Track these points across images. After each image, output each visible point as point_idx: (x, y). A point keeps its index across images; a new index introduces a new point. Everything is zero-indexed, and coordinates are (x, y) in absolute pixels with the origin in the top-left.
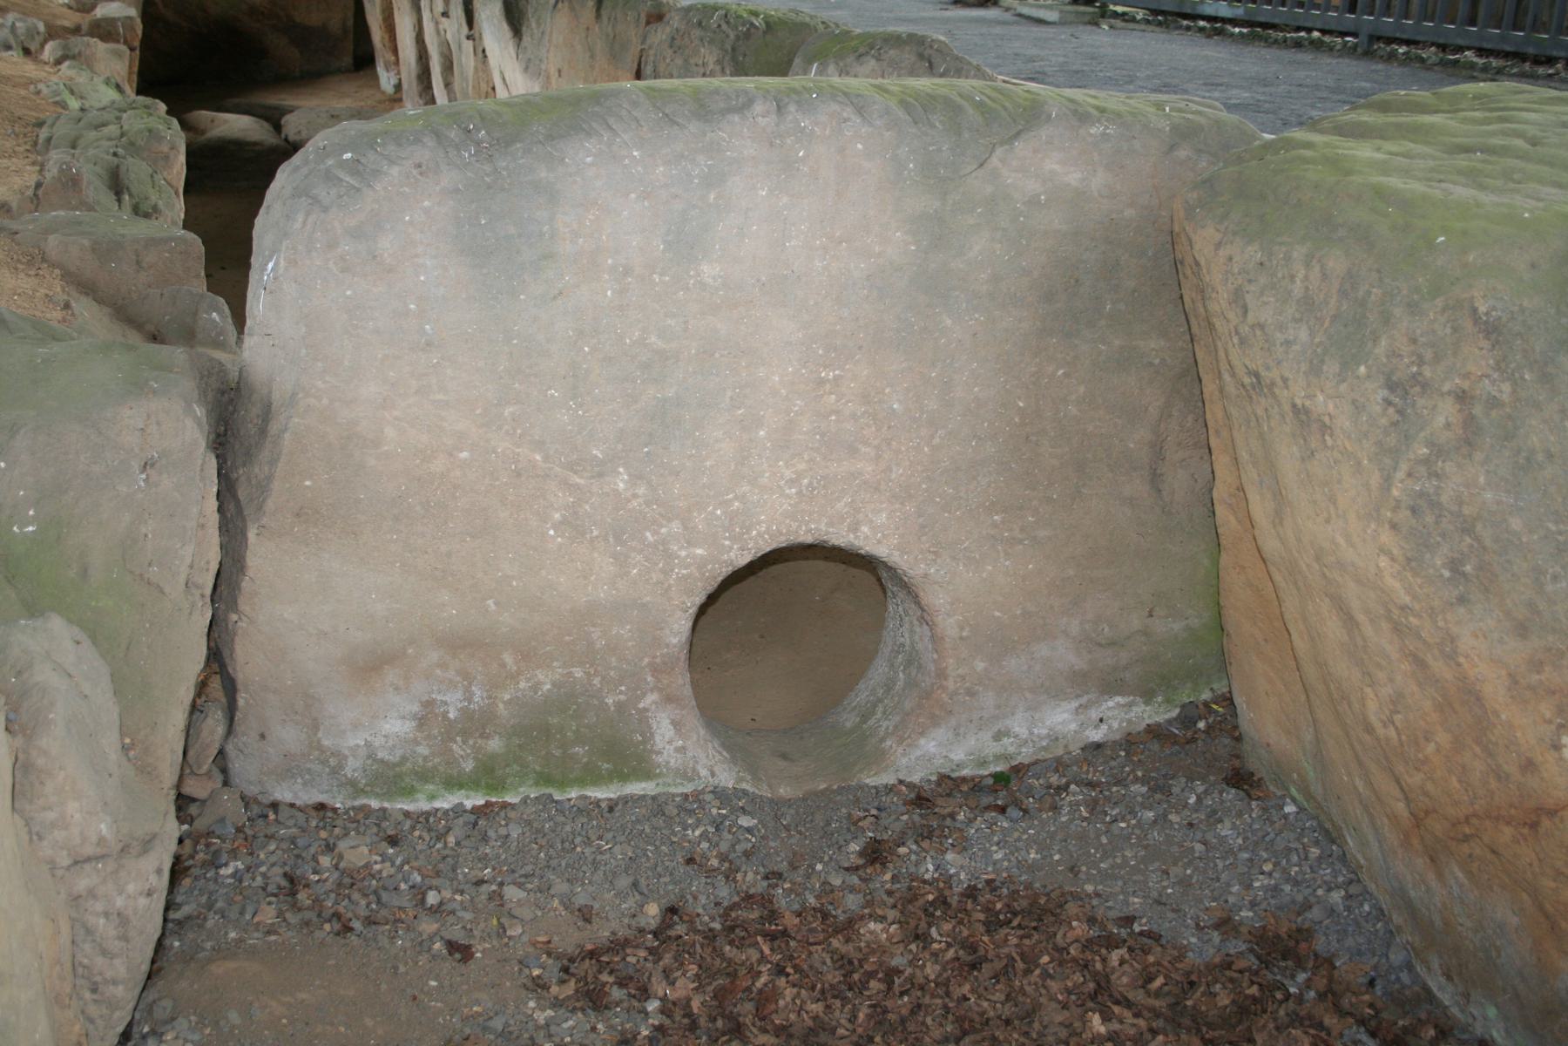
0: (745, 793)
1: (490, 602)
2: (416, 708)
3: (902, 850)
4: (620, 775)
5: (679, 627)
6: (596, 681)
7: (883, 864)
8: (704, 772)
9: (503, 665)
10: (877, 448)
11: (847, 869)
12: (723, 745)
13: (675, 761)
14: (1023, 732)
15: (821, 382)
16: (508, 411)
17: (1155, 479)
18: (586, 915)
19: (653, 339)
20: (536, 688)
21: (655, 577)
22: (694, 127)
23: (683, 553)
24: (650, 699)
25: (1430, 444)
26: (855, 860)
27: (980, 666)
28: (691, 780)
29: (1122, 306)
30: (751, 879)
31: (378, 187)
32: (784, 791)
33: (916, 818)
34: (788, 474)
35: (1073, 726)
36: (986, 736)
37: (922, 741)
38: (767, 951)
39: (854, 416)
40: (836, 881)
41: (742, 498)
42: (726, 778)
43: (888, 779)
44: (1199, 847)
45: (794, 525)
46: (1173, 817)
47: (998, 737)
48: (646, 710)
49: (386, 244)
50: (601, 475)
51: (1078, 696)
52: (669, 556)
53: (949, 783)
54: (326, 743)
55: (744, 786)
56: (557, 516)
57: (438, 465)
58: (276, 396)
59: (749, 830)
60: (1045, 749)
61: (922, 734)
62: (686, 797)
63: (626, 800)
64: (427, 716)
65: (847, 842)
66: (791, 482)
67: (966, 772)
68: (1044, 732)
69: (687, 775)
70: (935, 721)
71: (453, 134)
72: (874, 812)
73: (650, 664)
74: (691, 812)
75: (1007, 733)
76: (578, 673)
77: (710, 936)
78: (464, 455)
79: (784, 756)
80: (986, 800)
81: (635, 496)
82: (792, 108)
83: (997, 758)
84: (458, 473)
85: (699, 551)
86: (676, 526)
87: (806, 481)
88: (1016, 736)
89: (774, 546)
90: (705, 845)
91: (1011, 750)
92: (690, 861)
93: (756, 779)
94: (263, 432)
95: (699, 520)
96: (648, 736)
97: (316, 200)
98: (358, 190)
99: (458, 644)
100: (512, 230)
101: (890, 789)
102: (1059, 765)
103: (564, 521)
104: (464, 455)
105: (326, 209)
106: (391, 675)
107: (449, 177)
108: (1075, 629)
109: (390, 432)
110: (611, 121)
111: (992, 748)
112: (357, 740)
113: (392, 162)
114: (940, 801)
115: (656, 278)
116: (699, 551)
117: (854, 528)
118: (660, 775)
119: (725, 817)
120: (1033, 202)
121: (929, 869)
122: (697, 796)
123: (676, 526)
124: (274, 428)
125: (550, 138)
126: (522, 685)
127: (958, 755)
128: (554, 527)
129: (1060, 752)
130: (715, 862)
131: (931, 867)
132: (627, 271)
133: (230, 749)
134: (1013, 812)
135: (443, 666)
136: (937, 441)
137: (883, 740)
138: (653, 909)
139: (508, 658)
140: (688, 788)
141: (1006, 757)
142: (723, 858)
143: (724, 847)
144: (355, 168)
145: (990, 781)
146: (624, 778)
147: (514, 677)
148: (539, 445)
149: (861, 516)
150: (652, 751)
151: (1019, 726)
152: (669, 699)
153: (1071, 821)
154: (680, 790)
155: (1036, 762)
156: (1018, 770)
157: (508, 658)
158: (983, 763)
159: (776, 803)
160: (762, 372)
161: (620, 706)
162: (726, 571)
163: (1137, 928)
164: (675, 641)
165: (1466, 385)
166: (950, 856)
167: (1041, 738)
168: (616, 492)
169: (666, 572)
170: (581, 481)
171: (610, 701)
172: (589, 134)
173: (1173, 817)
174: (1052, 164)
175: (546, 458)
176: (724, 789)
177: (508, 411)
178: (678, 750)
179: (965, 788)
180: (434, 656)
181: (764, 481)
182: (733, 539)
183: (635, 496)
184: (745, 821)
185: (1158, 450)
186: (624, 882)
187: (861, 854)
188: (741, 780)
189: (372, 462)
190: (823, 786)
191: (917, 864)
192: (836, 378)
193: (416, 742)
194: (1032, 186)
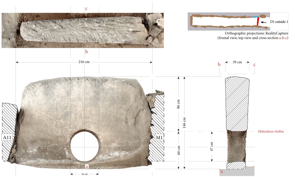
9: (48, 143)
10: (92, 118)
13: (69, 157)
17: (126, 122)
21: (66, 133)
24: (65, 148)
27: (106, 146)
29: (120, 101)
34: (81, 121)
35: (118, 155)
39: (88, 114)
41: (76, 123)
50: (59, 120)
51: (119, 151)
52: (67, 130)
56: (55, 125)
57: (42, 118)
58: (24, 110)
66: (81, 122)
73: (65, 144)
76: (57, 145)
78: (44, 117)
84: (43, 119)
86: (68, 126)
94: (23, 114)
96: (65, 153)
99: (43, 140)
100: (50, 92)
103: (55, 125)
104: (44, 117)
106: (35, 143)
107: (44, 86)
108: (117, 142)
109: (36, 114)
116: (71, 130)
120: (108, 89)
123: (68, 126)
124: (24, 114)
126: (50, 146)
128: (54, 126)
135: (41, 143)
147: (49, 144)
148: (53, 116)
150: (65, 155)
160: (78, 108)
162: (74, 132)
164: (68, 141)
168: (61, 122)
169: (67, 132)
174: (110, 85)
175: (53, 118)
177: (49, 112)
180: (40, 141)
182: (75, 128)
185: (126, 119)
189: (34, 117)
193: (38, 153)
194: (108, 88)
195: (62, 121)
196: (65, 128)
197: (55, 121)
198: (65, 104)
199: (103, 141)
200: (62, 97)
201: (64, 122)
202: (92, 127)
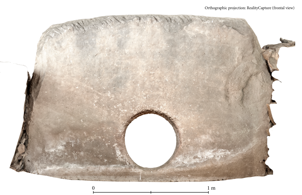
1: (82, 120)
9: (84, 135)
15: (150, 74)
19: (115, 64)
21: (116, 116)
23: (122, 111)
24: (115, 145)
27: (189, 140)
34: (144, 94)
35: (212, 156)
37: (177, 158)
41: (134, 99)
66: (145, 96)
76: (100, 137)
81: (112, 98)
86: (120, 105)
95: (126, 104)
96: (115, 153)
107: (76, 32)
115: (116, 52)
116: (126, 111)
123: (120, 105)
126: (88, 140)
136: (176, 88)
139: (85, 133)
149: (160, 104)
157: (85, 133)
164: (121, 131)
169: (119, 115)
170: (101, 94)
175: (94, 89)
183: (112, 98)
192: (153, 74)
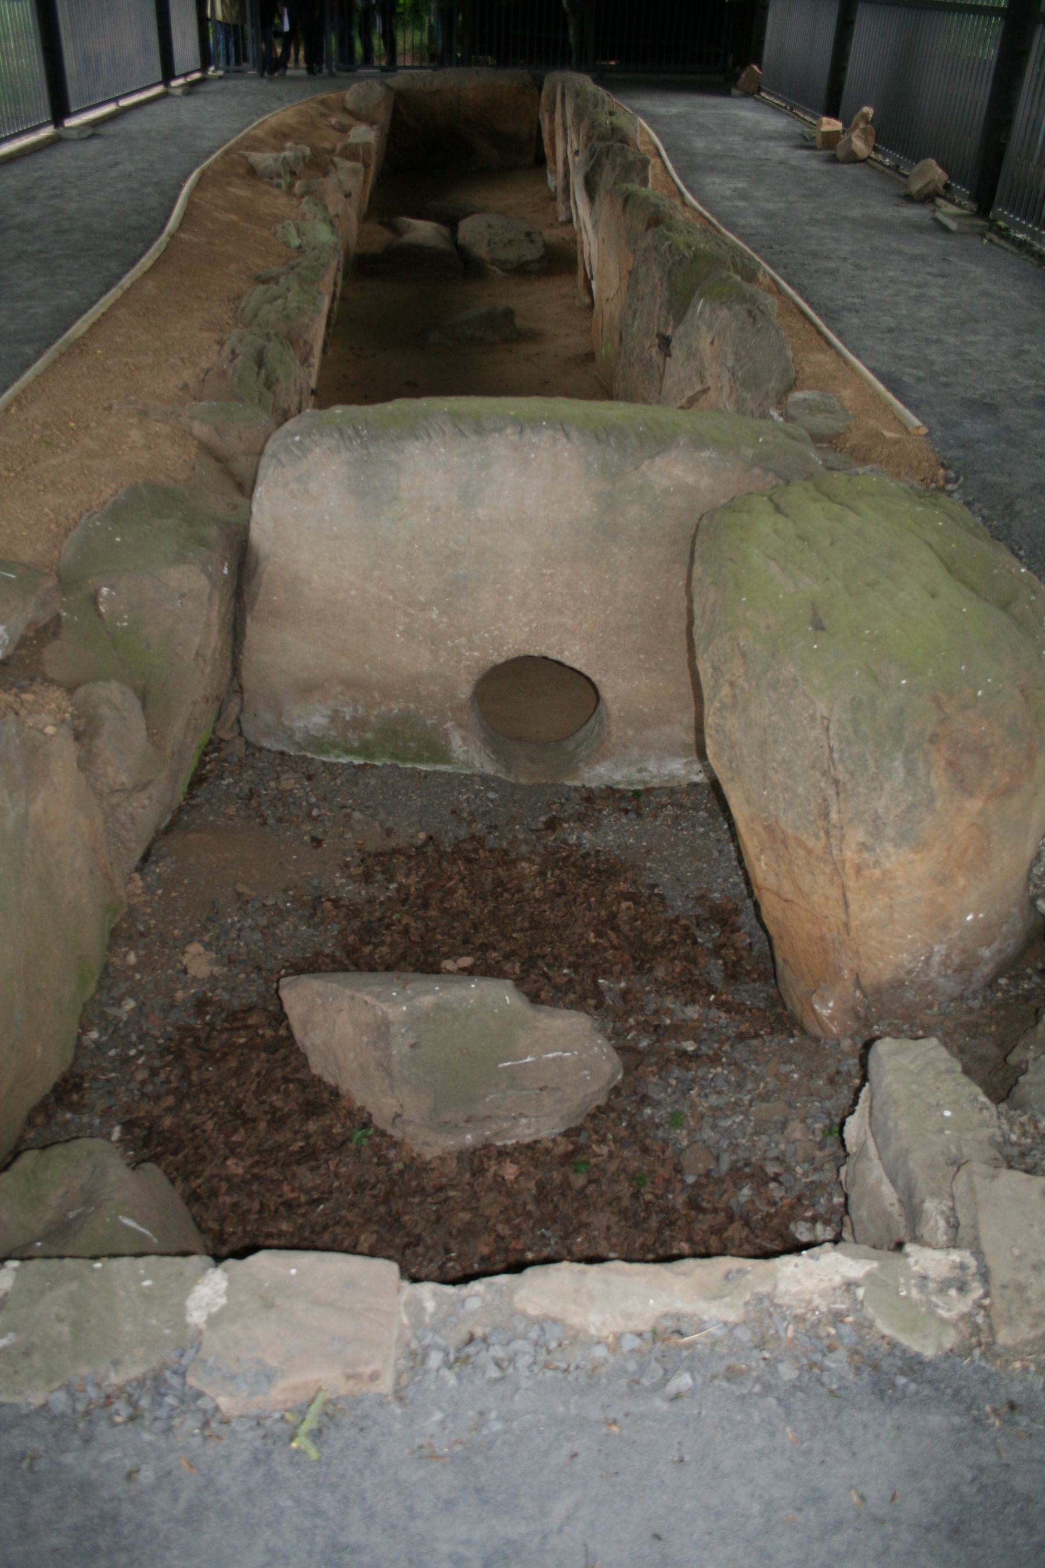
0: (498, 778)
1: (367, 666)
2: (329, 712)
3: (565, 825)
4: (435, 761)
5: (465, 691)
6: (421, 712)
7: (554, 831)
8: (478, 765)
9: (373, 697)
11: (532, 830)
12: (494, 752)
14: (655, 771)
15: (543, 575)
16: (376, 573)
18: (389, 832)
19: (451, 544)
20: (391, 710)
21: (452, 663)
22: (474, 438)
23: (467, 654)
24: (449, 725)
25: (721, 702)
26: (541, 826)
27: (630, 733)
28: (470, 768)
30: (479, 827)
31: (310, 457)
32: (523, 781)
33: (583, 808)
34: (525, 620)
35: (683, 772)
36: (634, 770)
37: (597, 767)
38: (462, 868)
40: (521, 837)
41: (499, 629)
42: (490, 769)
43: (577, 783)
44: (716, 854)
45: (528, 647)
46: (712, 834)
47: (640, 771)
48: (447, 729)
49: (314, 487)
50: (423, 610)
51: (686, 757)
53: (611, 792)
54: (286, 723)
55: (500, 775)
56: (401, 628)
59: (491, 801)
60: (667, 781)
61: (597, 763)
62: (466, 775)
63: (435, 773)
64: (335, 717)
65: (540, 815)
66: (526, 625)
67: (621, 786)
68: (666, 772)
69: (468, 765)
70: (604, 758)
71: (350, 431)
72: (563, 801)
74: (466, 785)
75: (645, 770)
76: (412, 706)
77: (442, 855)
79: (532, 761)
80: (623, 805)
81: (442, 622)
82: (528, 431)
83: (639, 782)
85: (476, 654)
86: (463, 640)
87: (534, 625)
88: (651, 772)
89: (517, 655)
90: (465, 805)
91: (648, 779)
92: (454, 812)
93: (509, 772)
95: (476, 638)
96: (448, 742)
97: (280, 461)
98: (300, 458)
101: (576, 789)
102: (672, 791)
104: (353, 592)
105: (284, 466)
107: (345, 455)
109: (315, 578)
110: (431, 432)
111: (636, 776)
112: (301, 724)
113: (317, 445)
114: (598, 802)
115: (453, 513)
116: (476, 654)
117: (561, 652)
118: (454, 763)
119: (481, 791)
121: (573, 839)
122: (473, 775)
123: (463, 640)
125: (399, 438)
126: (383, 708)
127: (617, 777)
128: (400, 632)
129: (675, 784)
130: (465, 815)
131: (575, 837)
132: (438, 509)
133: (241, 718)
134: (632, 815)
136: (608, 612)
137: (579, 762)
138: (422, 836)
139: (376, 695)
140: (469, 772)
141: (644, 782)
142: (471, 813)
143: (473, 807)
144: (299, 445)
145: (630, 794)
146: (436, 762)
149: (564, 646)
151: (652, 766)
152: (460, 726)
153: (660, 825)
154: (465, 772)
155: (659, 788)
156: (649, 791)
157: (376, 695)
158: (631, 783)
159: (515, 787)
161: (434, 726)
163: (656, 891)
164: (463, 697)
165: (733, 679)
166: (586, 834)
167: (665, 775)
169: (458, 662)
170: (413, 612)
171: (429, 722)
172: (417, 438)
173: (712, 834)
174: (678, 471)
175: (395, 598)
176: (488, 776)
178: (464, 752)
179: (617, 795)
181: (511, 622)
183: (442, 622)
184: (492, 795)
186: (414, 819)
187: (545, 823)
188: (498, 771)
190: (543, 781)
191: (569, 834)
192: (551, 575)
193: (329, 729)
195: (434, 616)
196: (449, 643)
197: (406, 613)
198: (451, 544)
199: (620, 711)
200: (438, 509)
201: (445, 620)
202: (576, 649)
